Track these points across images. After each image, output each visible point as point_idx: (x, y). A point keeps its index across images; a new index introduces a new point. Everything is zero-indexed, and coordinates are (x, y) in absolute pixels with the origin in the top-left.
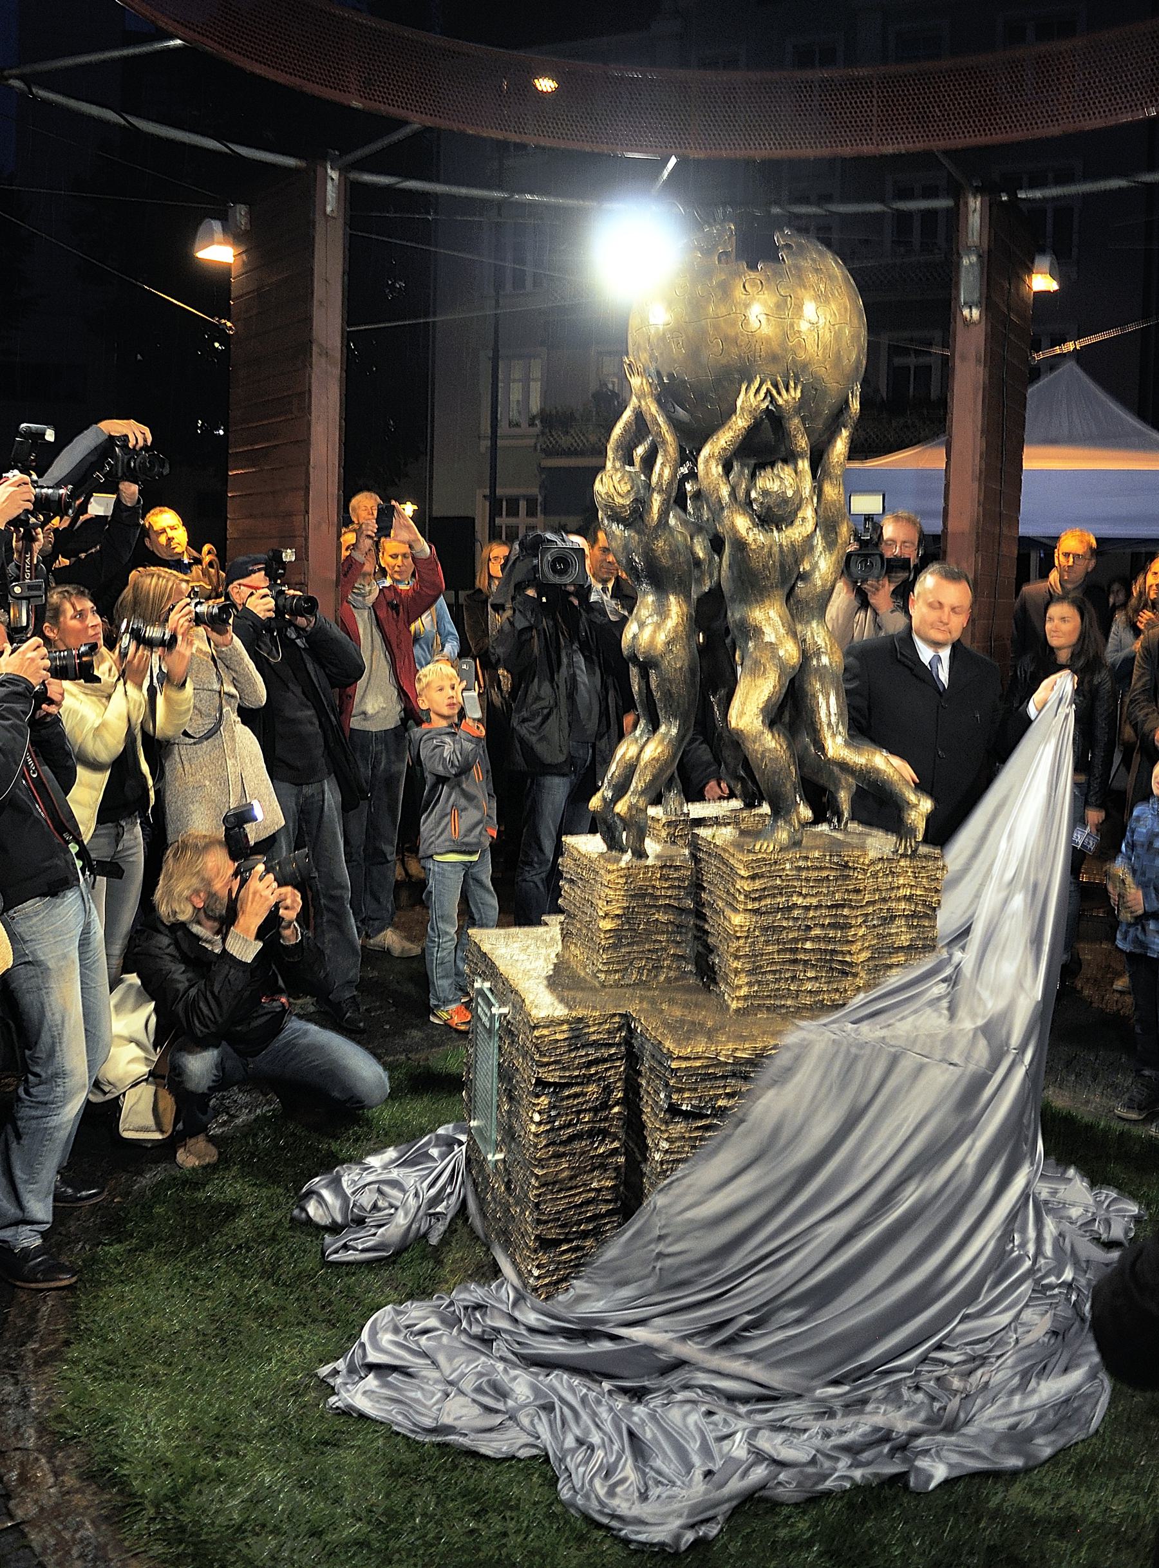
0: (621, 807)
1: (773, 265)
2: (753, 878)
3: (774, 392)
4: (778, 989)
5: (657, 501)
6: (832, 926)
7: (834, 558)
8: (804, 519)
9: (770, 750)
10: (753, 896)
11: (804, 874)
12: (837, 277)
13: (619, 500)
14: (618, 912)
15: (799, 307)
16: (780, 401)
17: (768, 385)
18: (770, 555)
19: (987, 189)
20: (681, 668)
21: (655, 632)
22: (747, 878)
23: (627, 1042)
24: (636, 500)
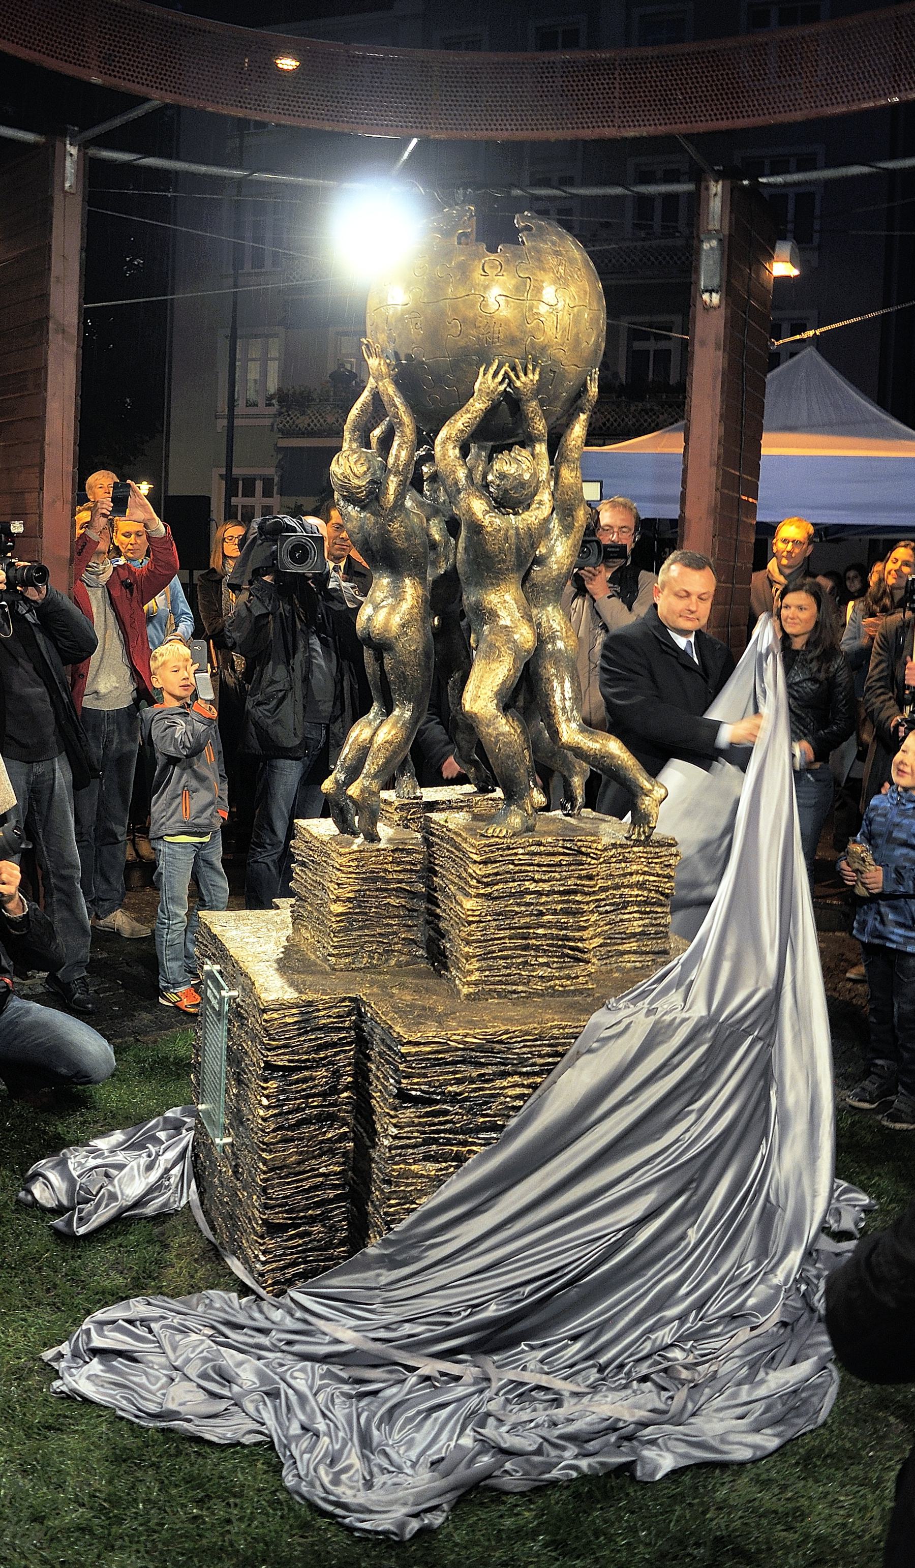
0: (354, 790)
1: (513, 247)
2: (485, 863)
3: (512, 374)
4: (509, 975)
5: (393, 483)
6: (565, 912)
7: (570, 541)
8: (540, 503)
9: (503, 734)
10: (485, 880)
11: (537, 860)
12: (576, 259)
13: (356, 482)
14: (351, 895)
15: (539, 290)
16: (518, 384)
17: (506, 367)
18: (506, 538)
19: (729, 174)
20: (415, 651)
21: (389, 614)
22: (480, 863)
23: (357, 1027)
24: (372, 482)
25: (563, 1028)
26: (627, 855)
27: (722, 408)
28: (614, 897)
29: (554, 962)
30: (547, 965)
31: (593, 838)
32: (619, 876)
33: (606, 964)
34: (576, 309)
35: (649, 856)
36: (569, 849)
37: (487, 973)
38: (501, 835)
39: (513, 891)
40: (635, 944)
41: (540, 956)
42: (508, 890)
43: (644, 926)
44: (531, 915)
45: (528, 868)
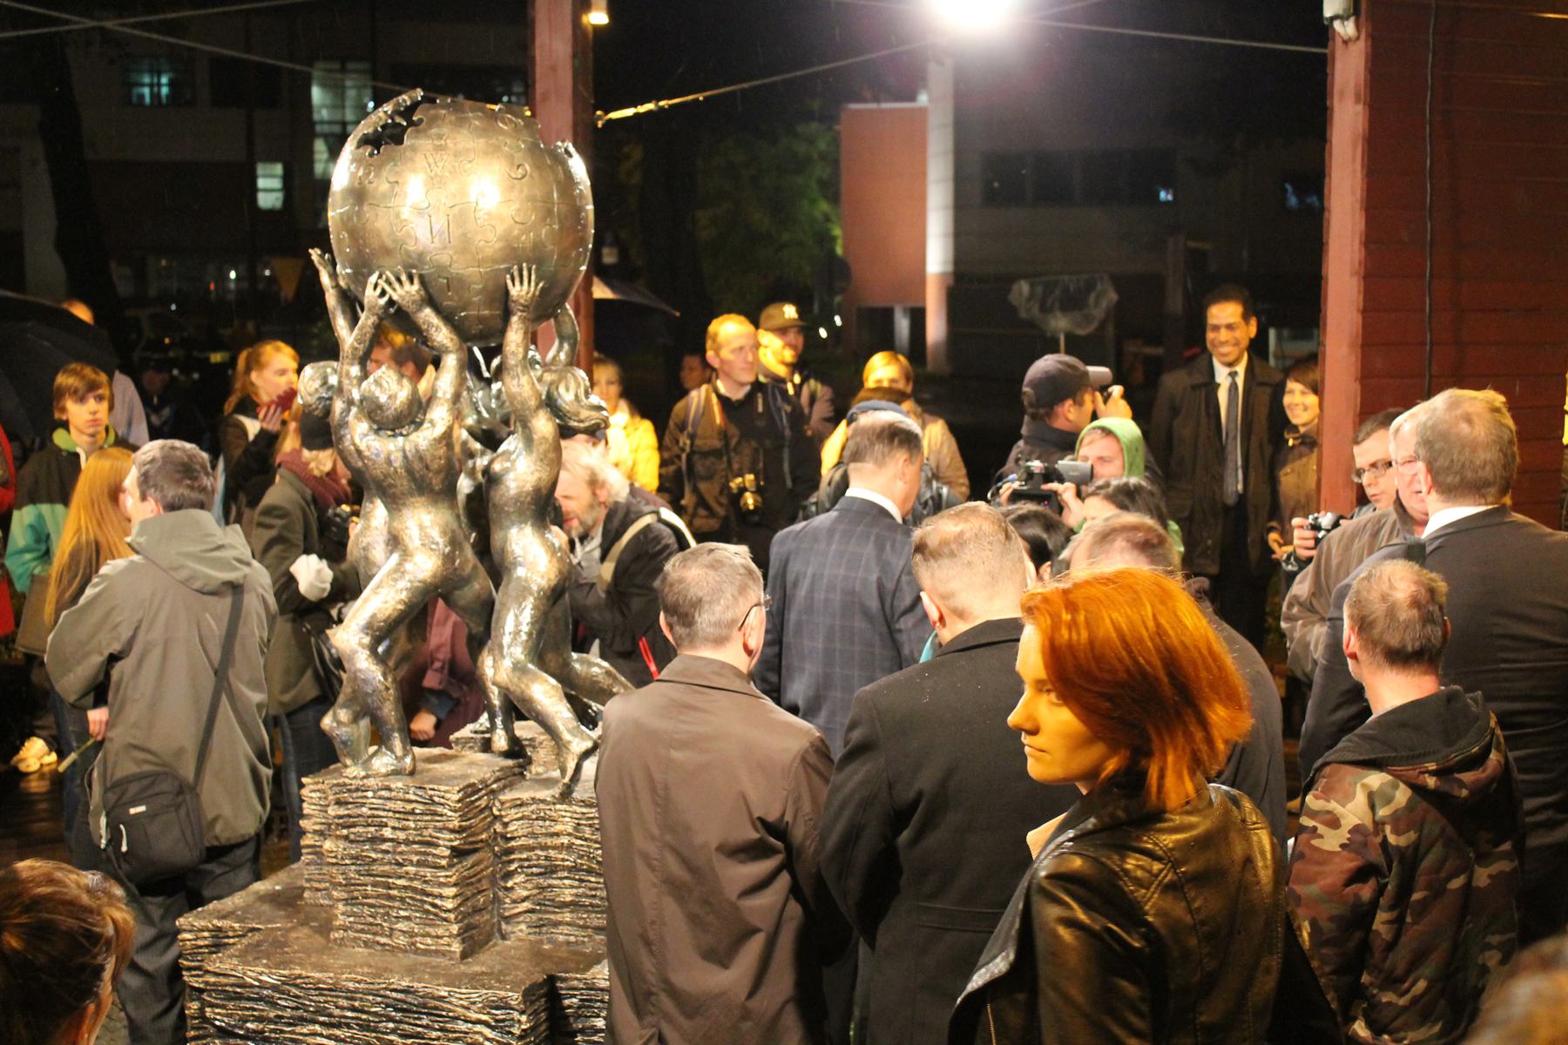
3: (387, 288)
4: (371, 924)
7: (534, 455)
8: (431, 422)
11: (390, 805)
14: (317, 827)
25: (359, 982)
27: (1362, 190)
30: (408, 918)
32: (546, 835)
34: (456, 209)
37: (352, 919)
43: (577, 895)
44: (390, 864)
45: (382, 813)
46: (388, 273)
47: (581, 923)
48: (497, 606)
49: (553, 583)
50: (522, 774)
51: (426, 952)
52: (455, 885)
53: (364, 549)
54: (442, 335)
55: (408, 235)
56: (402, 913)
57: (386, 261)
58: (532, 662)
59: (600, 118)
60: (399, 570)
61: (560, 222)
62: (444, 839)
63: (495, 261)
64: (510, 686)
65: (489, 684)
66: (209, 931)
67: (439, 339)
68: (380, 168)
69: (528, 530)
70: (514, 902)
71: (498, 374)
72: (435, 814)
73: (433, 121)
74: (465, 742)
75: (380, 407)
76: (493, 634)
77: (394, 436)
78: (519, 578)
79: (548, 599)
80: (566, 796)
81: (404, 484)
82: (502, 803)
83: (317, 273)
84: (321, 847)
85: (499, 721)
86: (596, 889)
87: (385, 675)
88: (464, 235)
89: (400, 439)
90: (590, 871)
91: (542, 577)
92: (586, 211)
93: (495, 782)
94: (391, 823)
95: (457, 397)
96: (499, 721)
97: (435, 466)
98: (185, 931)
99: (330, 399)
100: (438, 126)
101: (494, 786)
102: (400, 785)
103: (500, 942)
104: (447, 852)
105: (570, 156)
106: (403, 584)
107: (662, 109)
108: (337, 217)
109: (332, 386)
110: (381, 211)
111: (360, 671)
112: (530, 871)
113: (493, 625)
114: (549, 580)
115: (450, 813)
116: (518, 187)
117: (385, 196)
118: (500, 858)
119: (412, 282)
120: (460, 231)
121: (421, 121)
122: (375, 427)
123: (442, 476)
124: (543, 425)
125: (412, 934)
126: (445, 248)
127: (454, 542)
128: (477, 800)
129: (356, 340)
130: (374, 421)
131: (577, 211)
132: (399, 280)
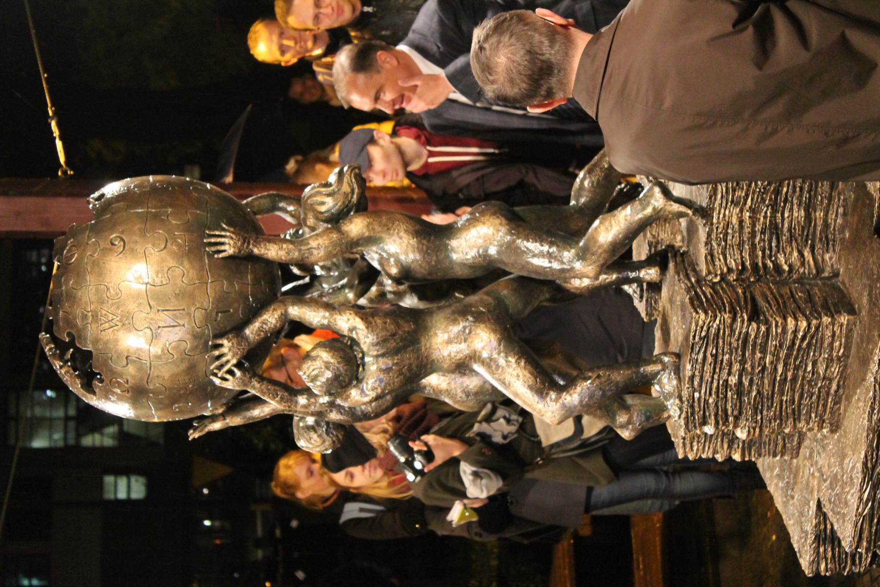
3: (226, 368)
4: (819, 397)
7: (383, 235)
8: (351, 330)
11: (707, 377)
14: (726, 446)
26: (720, 230)
28: (764, 240)
29: (814, 355)
30: (815, 363)
31: (693, 324)
33: (833, 246)
35: (724, 205)
36: (700, 348)
37: (813, 415)
38: (679, 413)
39: (735, 397)
40: (817, 214)
41: (806, 369)
42: (734, 401)
43: (799, 205)
44: (763, 377)
45: (715, 385)
46: (211, 368)
47: (826, 201)
48: (525, 274)
49: (504, 221)
50: (682, 255)
51: (847, 347)
52: (785, 319)
53: (468, 396)
54: (270, 318)
55: (176, 348)
56: (809, 368)
57: (201, 368)
58: (577, 243)
59: (64, 173)
60: (489, 364)
61: (165, 207)
62: (742, 327)
63: (202, 268)
64: (599, 263)
65: (597, 283)
66: (818, 547)
67: (274, 321)
68: (114, 373)
69: (454, 243)
70: (803, 264)
71: (307, 268)
72: (717, 335)
73: (70, 323)
74: (650, 308)
75: (336, 377)
76: (550, 278)
77: (364, 365)
78: (498, 252)
79: (518, 226)
80: (705, 213)
81: (408, 357)
82: (709, 273)
83: (211, 434)
84: (744, 442)
85: (632, 275)
86: (794, 187)
87: (586, 379)
88: (177, 296)
89: (367, 359)
90: (777, 192)
91: (498, 231)
92: (155, 182)
93: (689, 280)
94: (725, 377)
95: (329, 307)
96: (632, 275)
97: (392, 328)
98: (818, 568)
99: (328, 423)
100: (75, 319)
101: (693, 280)
102: (689, 367)
103: (840, 278)
104: (754, 325)
105: (103, 195)
106: (502, 361)
107: (55, 113)
108: (159, 413)
109: (316, 422)
110: (154, 373)
111: (581, 401)
112: (774, 249)
113: (542, 278)
114: (501, 224)
115: (717, 322)
116: (132, 245)
117: (140, 369)
118: (761, 276)
119: (221, 346)
120: (173, 300)
121: (69, 334)
122: (355, 382)
123: (401, 322)
124: (356, 227)
125: (830, 361)
126: (189, 314)
127: (464, 312)
128: (706, 297)
129: (274, 398)
130: (350, 383)
131: (154, 190)
132: (219, 357)
